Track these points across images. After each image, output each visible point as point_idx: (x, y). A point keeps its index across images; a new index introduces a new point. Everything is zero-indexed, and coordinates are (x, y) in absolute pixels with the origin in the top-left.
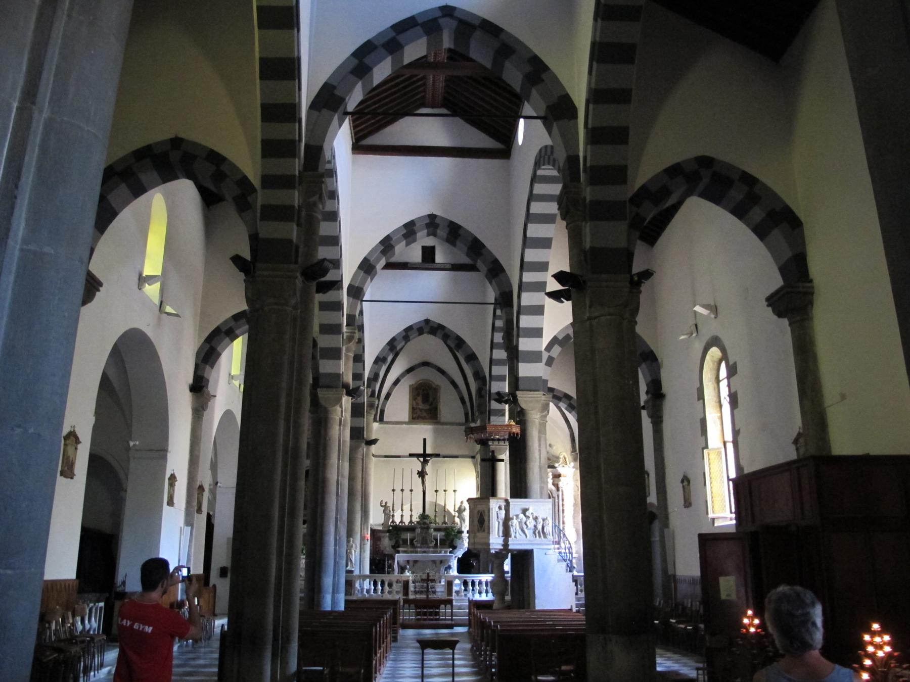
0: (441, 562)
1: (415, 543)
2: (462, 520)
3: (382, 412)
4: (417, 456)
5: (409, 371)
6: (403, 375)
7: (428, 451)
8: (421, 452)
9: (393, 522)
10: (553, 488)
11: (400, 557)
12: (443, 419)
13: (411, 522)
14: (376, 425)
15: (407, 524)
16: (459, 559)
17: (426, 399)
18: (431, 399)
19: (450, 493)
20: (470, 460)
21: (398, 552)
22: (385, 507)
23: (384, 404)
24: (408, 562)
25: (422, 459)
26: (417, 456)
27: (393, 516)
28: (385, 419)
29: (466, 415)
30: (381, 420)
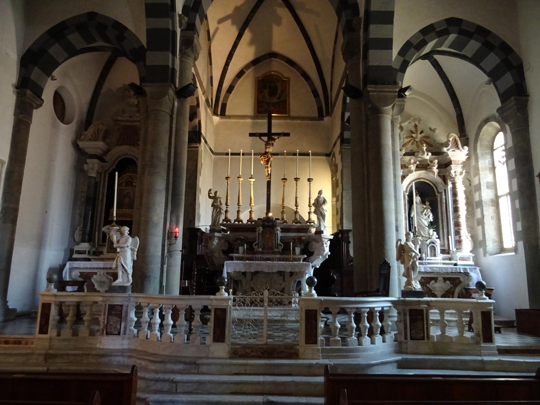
0: (292, 274)
1: (256, 247)
2: (321, 215)
3: (224, 106)
4: (261, 135)
5: (255, 62)
6: (247, 67)
7: (273, 131)
8: (266, 131)
9: (226, 220)
10: (439, 180)
11: (230, 268)
12: (293, 114)
13: (250, 220)
14: (216, 119)
15: (245, 222)
16: (316, 269)
17: (273, 93)
18: (279, 92)
19: (304, 182)
20: (324, 157)
21: (232, 259)
22: (215, 198)
23: (226, 98)
24: (244, 274)
25: (265, 138)
26: (261, 135)
27: (226, 212)
28: (227, 114)
29: (320, 109)
30: (223, 114)
